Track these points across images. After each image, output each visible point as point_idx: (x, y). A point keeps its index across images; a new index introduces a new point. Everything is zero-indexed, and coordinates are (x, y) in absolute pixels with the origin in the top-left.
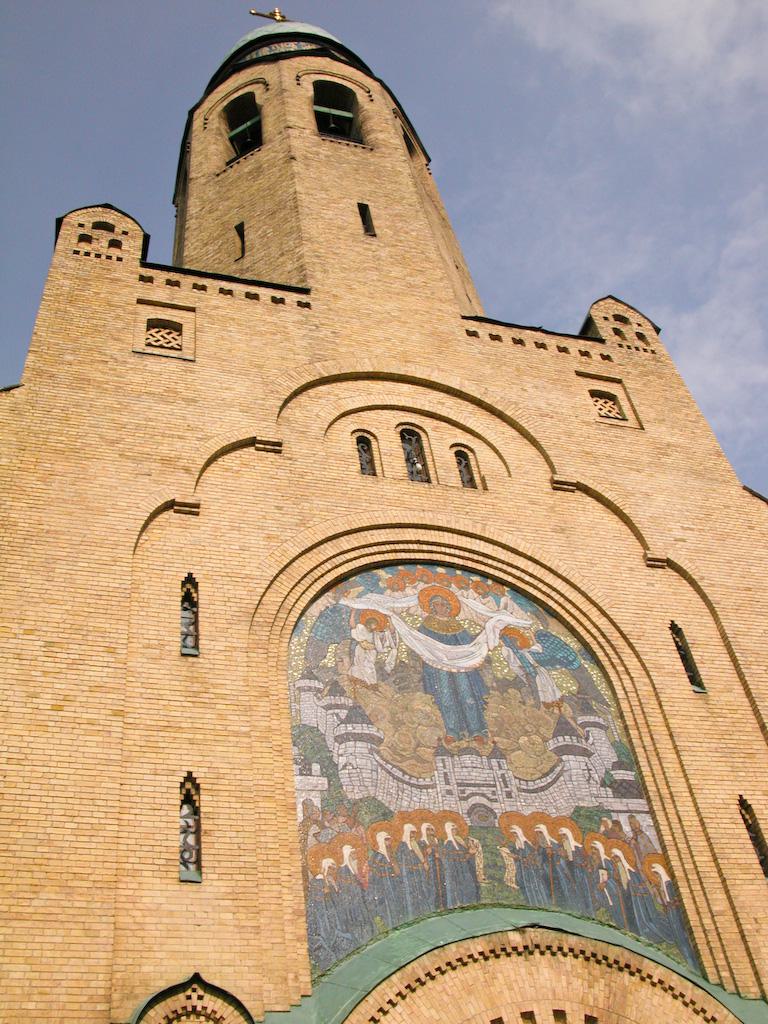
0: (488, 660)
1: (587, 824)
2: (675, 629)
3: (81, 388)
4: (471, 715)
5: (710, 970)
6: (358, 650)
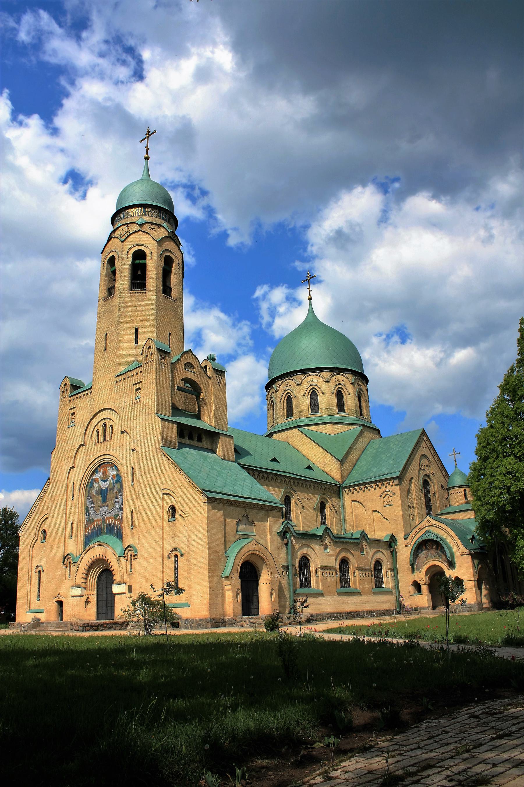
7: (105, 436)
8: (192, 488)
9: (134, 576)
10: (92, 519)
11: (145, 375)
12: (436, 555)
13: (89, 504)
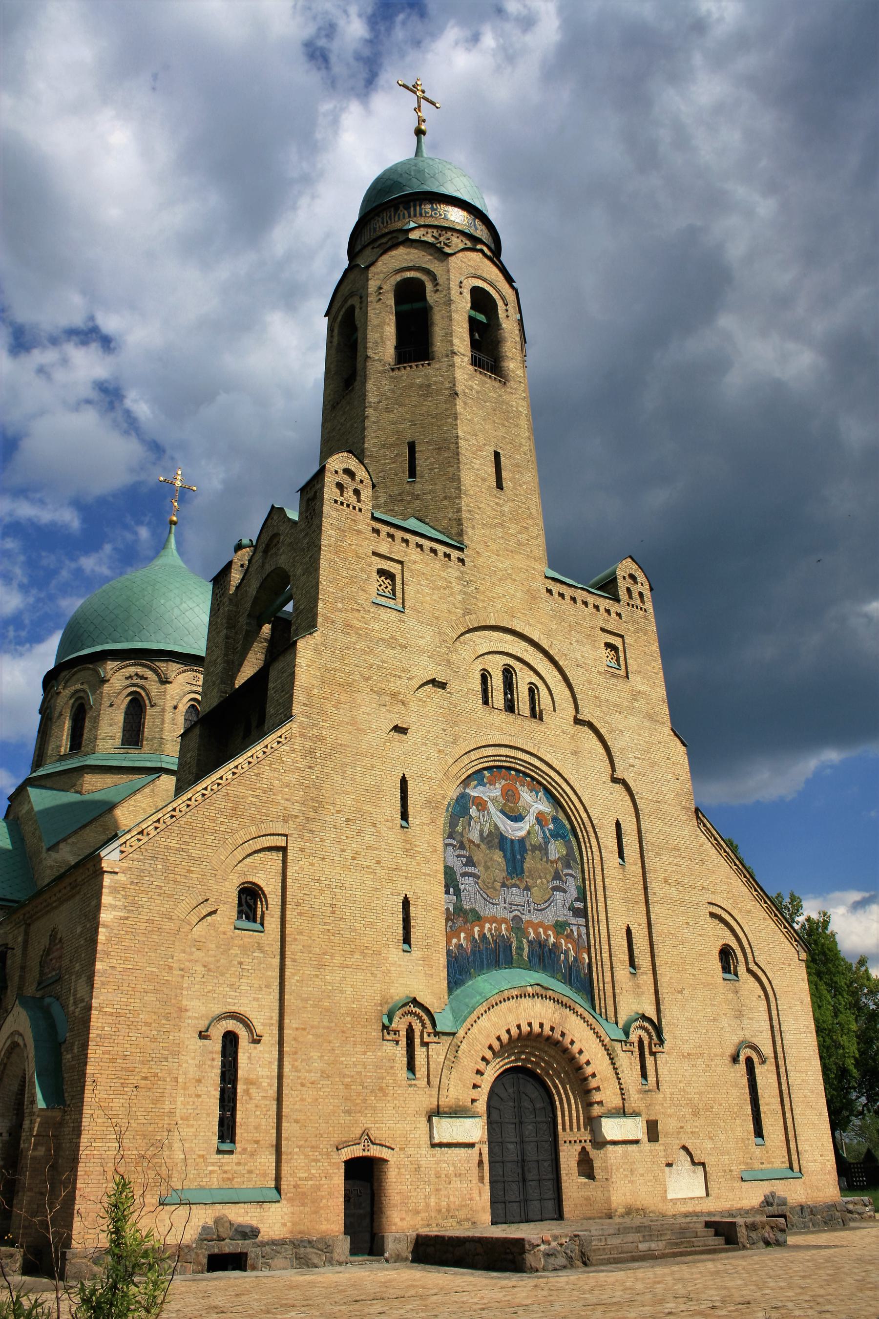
0: (529, 833)
1: (559, 930)
3: (348, 634)
4: (518, 864)
5: (597, 1007)
6: (472, 822)
9: (660, 1096)
10: (473, 910)
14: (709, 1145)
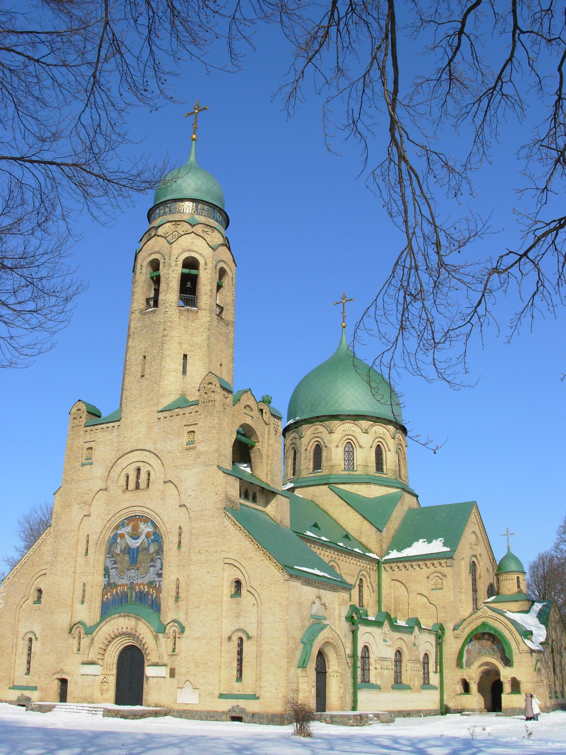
0: (141, 543)
2: (180, 528)
4: (135, 559)
7: (137, 483)
8: (267, 562)
9: (179, 658)
10: (114, 583)
11: (202, 416)
12: (491, 650)
13: (109, 564)
14: (202, 681)
